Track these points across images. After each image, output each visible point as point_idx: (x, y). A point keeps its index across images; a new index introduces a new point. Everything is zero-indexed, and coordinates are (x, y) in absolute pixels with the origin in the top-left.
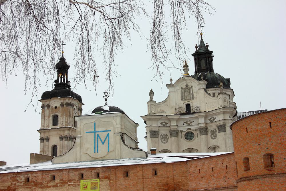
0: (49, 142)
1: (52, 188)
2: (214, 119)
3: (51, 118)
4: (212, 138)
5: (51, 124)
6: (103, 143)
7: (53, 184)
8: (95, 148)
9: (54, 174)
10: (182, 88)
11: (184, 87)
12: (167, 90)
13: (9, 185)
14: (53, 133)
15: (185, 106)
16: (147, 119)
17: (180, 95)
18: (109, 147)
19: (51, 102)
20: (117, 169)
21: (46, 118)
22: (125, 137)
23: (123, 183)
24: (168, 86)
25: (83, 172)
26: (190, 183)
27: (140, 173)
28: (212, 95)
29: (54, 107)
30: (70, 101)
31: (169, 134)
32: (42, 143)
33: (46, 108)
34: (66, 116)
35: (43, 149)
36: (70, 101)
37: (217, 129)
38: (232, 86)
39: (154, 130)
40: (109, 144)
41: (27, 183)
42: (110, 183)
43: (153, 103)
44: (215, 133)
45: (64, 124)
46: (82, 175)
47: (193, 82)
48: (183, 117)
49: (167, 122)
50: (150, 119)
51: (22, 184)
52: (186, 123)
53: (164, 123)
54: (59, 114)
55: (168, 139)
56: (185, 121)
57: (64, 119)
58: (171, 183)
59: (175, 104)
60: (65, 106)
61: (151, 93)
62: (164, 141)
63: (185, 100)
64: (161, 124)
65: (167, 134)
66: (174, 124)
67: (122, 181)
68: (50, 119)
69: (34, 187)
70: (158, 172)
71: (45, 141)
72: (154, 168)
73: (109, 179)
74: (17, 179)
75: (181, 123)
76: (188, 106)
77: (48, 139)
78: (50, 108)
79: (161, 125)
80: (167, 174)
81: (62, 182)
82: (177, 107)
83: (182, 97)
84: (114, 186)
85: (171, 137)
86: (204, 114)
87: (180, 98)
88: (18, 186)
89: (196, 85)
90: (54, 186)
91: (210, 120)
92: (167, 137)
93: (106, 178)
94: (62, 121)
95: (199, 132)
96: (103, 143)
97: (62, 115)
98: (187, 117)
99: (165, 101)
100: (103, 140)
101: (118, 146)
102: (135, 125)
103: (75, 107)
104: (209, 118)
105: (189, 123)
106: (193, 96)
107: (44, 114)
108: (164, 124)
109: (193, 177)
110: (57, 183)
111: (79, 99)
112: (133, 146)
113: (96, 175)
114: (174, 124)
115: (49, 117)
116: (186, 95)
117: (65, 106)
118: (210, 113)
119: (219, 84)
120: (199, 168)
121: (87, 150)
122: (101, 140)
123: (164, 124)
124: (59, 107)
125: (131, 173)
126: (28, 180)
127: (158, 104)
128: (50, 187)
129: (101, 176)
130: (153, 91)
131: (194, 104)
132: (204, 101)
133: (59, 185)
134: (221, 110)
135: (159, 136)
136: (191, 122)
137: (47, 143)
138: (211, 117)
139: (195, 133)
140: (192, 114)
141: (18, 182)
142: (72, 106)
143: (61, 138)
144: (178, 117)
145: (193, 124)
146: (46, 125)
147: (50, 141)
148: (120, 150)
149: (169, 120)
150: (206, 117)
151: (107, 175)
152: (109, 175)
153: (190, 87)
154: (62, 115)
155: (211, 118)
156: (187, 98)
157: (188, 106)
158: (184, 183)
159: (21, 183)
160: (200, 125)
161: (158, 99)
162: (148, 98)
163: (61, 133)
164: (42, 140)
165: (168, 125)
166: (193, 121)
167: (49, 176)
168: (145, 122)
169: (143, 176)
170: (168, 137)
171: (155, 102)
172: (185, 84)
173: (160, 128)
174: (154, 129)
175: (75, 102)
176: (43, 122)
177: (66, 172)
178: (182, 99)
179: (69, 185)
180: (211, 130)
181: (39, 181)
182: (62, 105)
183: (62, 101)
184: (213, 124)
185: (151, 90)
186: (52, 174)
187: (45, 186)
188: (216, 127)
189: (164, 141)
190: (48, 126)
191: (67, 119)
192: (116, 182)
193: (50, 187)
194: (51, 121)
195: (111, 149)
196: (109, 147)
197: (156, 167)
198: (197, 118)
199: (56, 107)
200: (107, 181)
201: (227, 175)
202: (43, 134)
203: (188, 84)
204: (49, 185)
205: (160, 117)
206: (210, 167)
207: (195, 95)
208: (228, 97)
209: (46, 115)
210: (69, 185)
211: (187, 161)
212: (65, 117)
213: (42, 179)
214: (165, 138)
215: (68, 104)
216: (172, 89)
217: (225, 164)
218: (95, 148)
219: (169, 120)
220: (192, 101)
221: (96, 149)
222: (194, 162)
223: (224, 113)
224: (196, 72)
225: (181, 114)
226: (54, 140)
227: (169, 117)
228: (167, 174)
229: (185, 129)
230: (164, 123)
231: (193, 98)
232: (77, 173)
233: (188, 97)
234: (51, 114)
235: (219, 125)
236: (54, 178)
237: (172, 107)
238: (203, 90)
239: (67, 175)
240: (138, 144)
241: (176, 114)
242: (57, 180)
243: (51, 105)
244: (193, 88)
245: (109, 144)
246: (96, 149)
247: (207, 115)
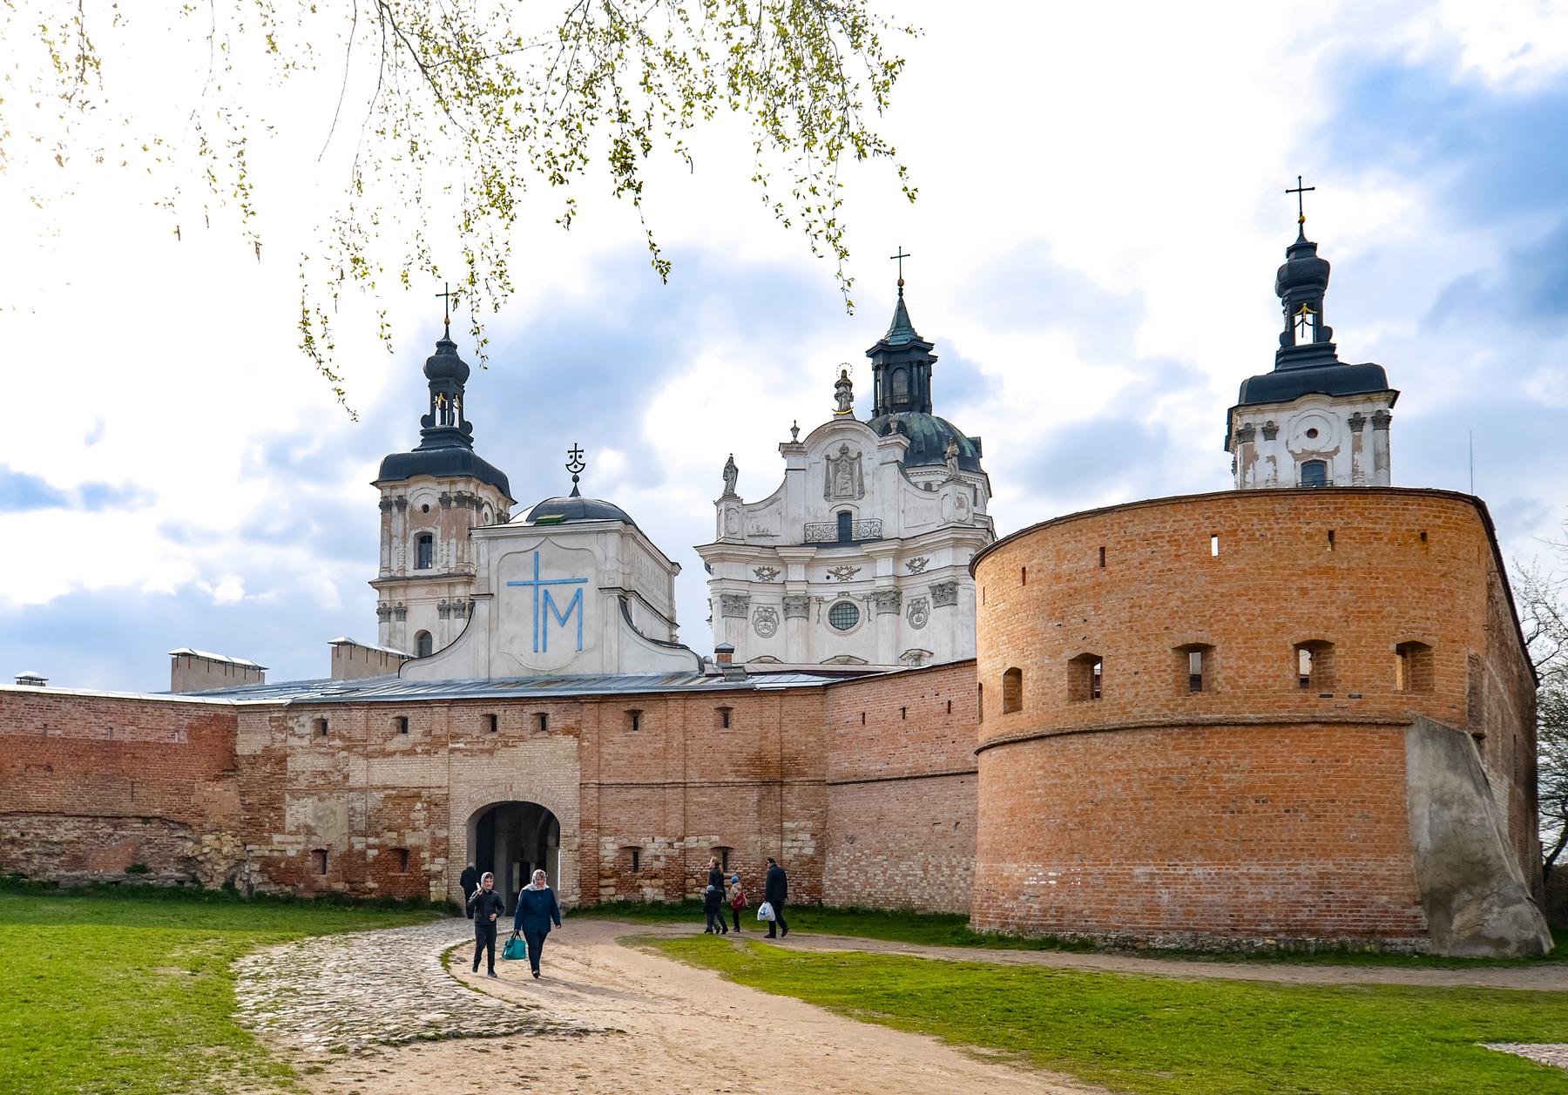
1: (397, 756)
2: (923, 565)
3: (411, 544)
5: (410, 565)
6: (563, 621)
7: (403, 747)
8: (536, 636)
9: (403, 713)
10: (828, 458)
11: (835, 454)
12: (783, 464)
13: (268, 743)
14: (416, 592)
15: (835, 518)
16: (713, 555)
17: (821, 482)
18: (580, 634)
20: (603, 706)
21: (395, 542)
22: (634, 604)
23: (622, 750)
24: (787, 449)
25: (495, 711)
26: (832, 756)
27: (676, 720)
28: (922, 486)
29: (418, 506)
30: (472, 488)
32: (386, 624)
33: (395, 510)
34: (459, 537)
36: (472, 488)
38: (984, 464)
39: (734, 593)
40: (580, 624)
41: (319, 740)
42: (580, 747)
43: (733, 505)
45: (453, 564)
46: (493, 718)
47: (863, 441)
48: (825, 554)
49: (776, 569)
50: (722, 558)
51: (305, 742)
53: (766, 572)
54: (437, 533)
56: (834, 569)
57: (453, 547)
58: (773, 755)
59: (802, 511)
60: (454, 504)
61: (731, 470)
63: (837, 498)
64: (758, 573)
66: (797, 573)
67: (619, 744)
69: (345, 753)
70: (734, 716)
71: (393, 616)
72: (720, 705)
73: (577, 736)
74: (291, 724)
75: (820, 574)
76: (845, 517)
77: (402, 612)
79: (756, 579)
80: (761, 727)
81: (428, 739)
82: (811, 520)
83: (827, 487)
84: (595, 759)
88: (292, 748)
89: (875, 449)
90: (404, 753)
91: (910, 566)
93: (568, 731)
94: (445, 556)
96: (563, 621)
97: (446, 535)
99: (772, 500)
100: (562, 610)
101: (612, 631)
102: (668, 566)
103: (486, 509)
105: (844, 574)
106: (861, 485)
108: (765, 576)
109: (842, 736)
110: (415, 745)
111: (498, 482)
112: (662, 633)
113: (538, 722)
114: (797, 573)
115: (405, 539)
116: (839, 480)
117: (454, 504)
118: (912, 544)
119: (945, 454)
120: (861, 708)
121: (511, 641)
122: (556, 611)
123: (765, 576)
124: (436, 509)
125: (648, 719)
126: (322, 726)
127: (752, 508)
128: (394, 753)
129: (551, 724)
130: (736, 463)
131: (865, 513)
132: (892, 500)
133: (419, 749)
134: (947, 535)
135: (753, 608)
136: (851, 573)
137: (400, 624)
140: (858, 543)
141: (294, 735)
142: (478, 504)
143: (444, 610)
144: (810, 552)
145: (856, 577)
146: (395, 567)
147: (408, 616)
148: (615, 645)
149: (783, 562)
150: (898, 555)
151: (571, 722)
152: (578, 722)
154: (446, 535)
157: (845, 517)
158: (812, 755)
159: (301, 737)
160: (879, 583)
161: (751, 490)
162: (719, 488)
163: (443, 593)
164: (384, 613)
165: (778, 579)
167: (388, 721)
168: (708, 568)
169: (685, 731)
171: (739, 500)
173: (753, 588)
174: (733, 589)
175: (486, 494)
176: (386, 557)
177: (441, 711)
178: (827, 495)
179: (452, 751)
181: (358, 734)
182: (445, 500)
183: (446, 488)
184: (918, 580)
186: (398, 714)
187: (374, 751)
190: (404, 570)
192: (600, 745)
193: (394, 753)
195: (588, 640)
196: (580, 634)
197: (728, 702)
198: (870, 558)
199: (426, 508)
200: (570, 742)
201: (948, 732)
202: (386, 597)
204: (390, 747)
205: (754, 552)
206: (898, 706)
207: (867, 481)
208: (969, 493)
209: (394, 533)
210: (452, 751)
211: (826, 687)
212: (453, 541)
213: (368, 729)
214: (767, 616)
215: (463, 500)
216: (799, 462)
217: (944, 697)
218: (536, 636)
219: (783, 562)
220: (858, 503)
221: (540, 642)
222: (848, 690)
223: (957, 543)
224: (876, 412)
225: (820, 545)
226: (424, 615)
227: (783, 553)
228: (761, 727)
230: (766, 572)
231: (862, 493)
232: (477, 713)
235: (936, 583)
236: (403, 726)
237: (795, 520)
238: (895, 467)
239: (444, 719)
240: (678, 632)
241: (806, 544)
242: (415, 735)
245: (580, 624)
246: (540, 642)
247: (904, 549)
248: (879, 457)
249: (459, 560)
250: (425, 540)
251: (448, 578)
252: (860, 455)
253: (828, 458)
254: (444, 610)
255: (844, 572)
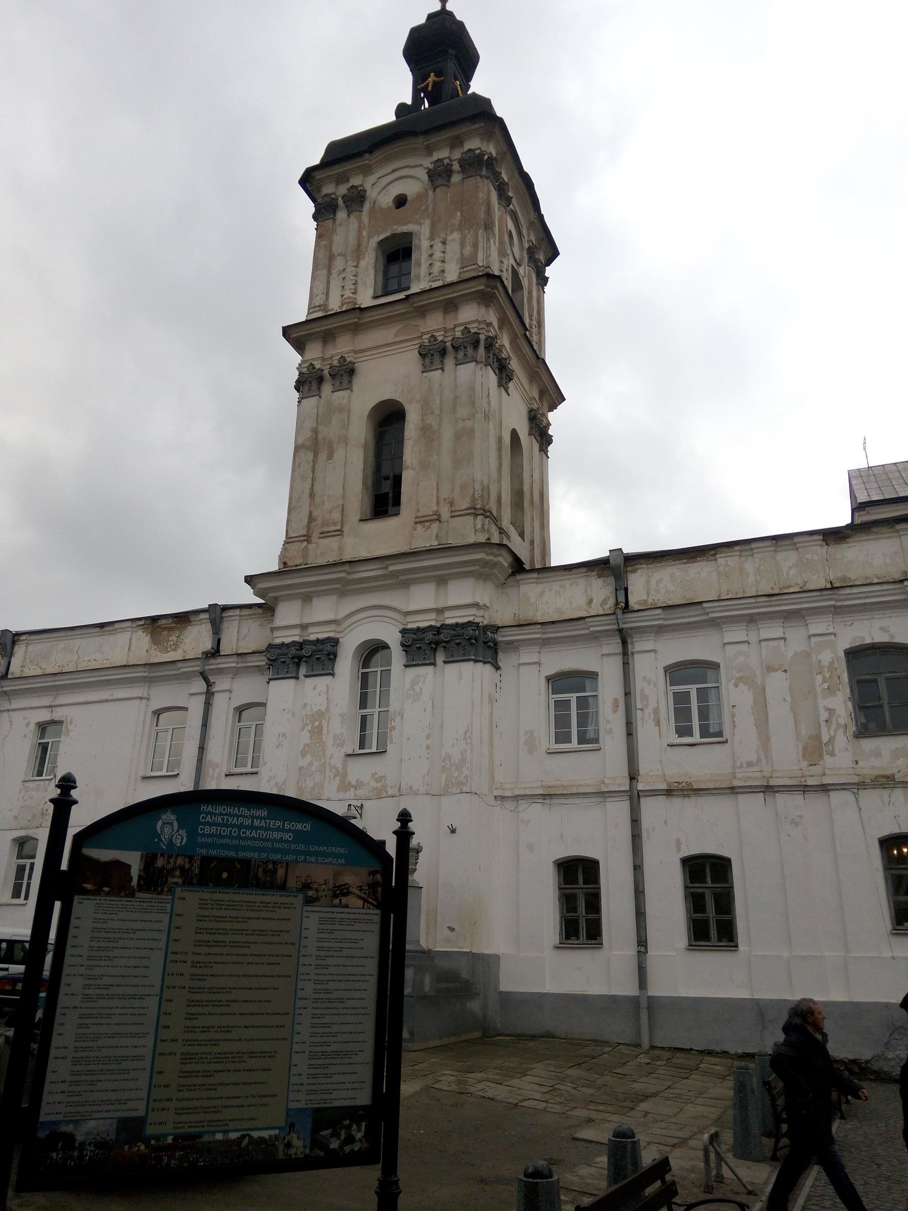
0: (356, 387)
19: (372, 179)
21: (339, 263)
29: (387, 200)
32: (311, 402)
35: (315, 431)
54: (422, 232)
57: (453, 250)
68: (363, 264)
78: (367, 206)
94: (438, 261)
107: (331, 241)
117: (456, 178)
124: (421, 197)
137: (341, 396)
143: (433, 354)
176: (321, 288)
182: (439, 175)
191: (469, 239)
194: (372, 272)
199: (401, 201)
209: (336, 249)
234: (370, 237)
243: (372, 193)
249: (465, 262)
250: (397, 254)
251: (446, 298)
254: (433, 354)
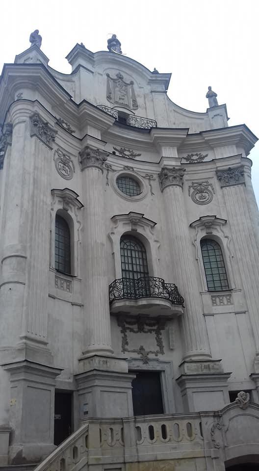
4: (196, 201)
10: (108, 75)
31: (75, 160)
37: (215, 182)
44: (207, 189)
49: (73, 128)
52: (120, 153)
55: (73, 171)
56: (119, 148)
62: (63, 172)
63: (117, 102)
65: (71, 157)
85: (82, 170)
86: (182, 135)
87: (105, 95)
92: (71, 164)
95: (156, 184)
98: (128, 135)
104: (185, 156)
106: (134, 101)
138: (190, 154)
139: (145, 183)
153: (128, 82)
155: (192, 155)
156: (121, 101)
166: (139, 155)
170: (73, 165)
172: (117, 72)
180: (193, 183)
185: (37, 31)
188: (212, 174)
189: (63, 172)
203: (122, 73)
207: (140, 101)
229: (118, 165)
231: (136, 106)
233: (123, 99)
244: (135, 86)
248: (147, 89)
252: (132, 83)
253: (108, 75)
255: (127, 153)
